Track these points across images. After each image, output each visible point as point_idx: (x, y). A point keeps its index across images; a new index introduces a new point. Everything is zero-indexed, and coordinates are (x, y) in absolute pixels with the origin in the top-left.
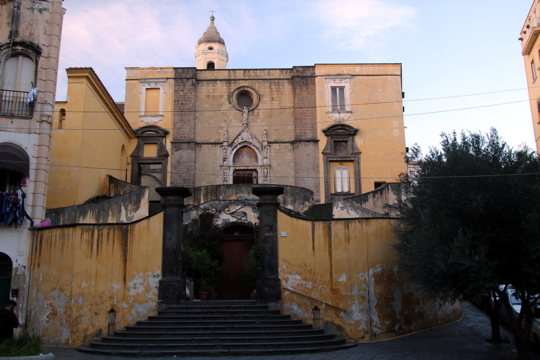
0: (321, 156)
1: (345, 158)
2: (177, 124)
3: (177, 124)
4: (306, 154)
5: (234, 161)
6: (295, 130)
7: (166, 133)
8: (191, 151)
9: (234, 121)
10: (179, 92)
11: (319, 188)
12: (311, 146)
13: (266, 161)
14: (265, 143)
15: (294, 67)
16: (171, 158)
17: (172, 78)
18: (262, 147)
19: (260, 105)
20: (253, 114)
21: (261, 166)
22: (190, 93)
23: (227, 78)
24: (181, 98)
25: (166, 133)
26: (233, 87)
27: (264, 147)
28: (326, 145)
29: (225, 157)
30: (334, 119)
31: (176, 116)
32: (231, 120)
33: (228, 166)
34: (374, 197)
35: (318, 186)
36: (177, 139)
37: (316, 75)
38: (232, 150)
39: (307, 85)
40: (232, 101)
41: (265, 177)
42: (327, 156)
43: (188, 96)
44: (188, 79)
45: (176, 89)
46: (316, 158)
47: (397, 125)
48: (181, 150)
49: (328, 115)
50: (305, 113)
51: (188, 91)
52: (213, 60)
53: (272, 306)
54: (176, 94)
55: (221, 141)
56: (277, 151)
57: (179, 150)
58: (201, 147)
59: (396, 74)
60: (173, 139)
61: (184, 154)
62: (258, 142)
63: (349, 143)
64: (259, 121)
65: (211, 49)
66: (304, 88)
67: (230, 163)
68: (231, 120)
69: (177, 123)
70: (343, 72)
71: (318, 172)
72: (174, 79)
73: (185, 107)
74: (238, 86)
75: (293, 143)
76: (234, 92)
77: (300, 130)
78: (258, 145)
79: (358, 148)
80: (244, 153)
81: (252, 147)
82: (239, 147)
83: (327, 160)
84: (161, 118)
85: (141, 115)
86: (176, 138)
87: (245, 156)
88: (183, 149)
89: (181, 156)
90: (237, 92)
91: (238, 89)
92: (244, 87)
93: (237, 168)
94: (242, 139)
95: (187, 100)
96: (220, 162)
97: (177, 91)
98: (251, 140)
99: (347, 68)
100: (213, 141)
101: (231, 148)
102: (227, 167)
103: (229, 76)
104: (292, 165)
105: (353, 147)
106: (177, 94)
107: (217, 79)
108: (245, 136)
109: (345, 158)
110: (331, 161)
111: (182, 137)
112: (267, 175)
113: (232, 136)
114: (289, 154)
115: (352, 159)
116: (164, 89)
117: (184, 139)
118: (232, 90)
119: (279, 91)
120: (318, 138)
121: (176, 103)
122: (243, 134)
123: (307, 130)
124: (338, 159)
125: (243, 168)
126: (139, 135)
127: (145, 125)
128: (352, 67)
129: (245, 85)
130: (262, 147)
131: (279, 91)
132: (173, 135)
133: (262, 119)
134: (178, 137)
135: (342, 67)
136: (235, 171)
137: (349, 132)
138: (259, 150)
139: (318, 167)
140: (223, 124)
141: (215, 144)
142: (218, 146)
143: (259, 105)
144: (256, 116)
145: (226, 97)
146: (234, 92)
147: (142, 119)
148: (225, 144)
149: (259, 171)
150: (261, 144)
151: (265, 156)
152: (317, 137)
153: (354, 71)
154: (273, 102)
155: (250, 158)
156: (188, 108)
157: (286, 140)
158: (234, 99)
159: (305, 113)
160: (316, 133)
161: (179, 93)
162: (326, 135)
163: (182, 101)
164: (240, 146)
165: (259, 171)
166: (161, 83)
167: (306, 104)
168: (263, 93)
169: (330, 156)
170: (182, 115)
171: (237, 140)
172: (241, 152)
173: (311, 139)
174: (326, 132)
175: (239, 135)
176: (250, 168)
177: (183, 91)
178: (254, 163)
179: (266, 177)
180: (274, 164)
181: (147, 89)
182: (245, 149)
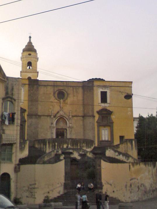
0: (96, 124)
16: (27, 122)
26: (56, 89)
38: (56, 119)
46: (93, 124)
52: (31, 61)
63: (109, 118)
65: (30, 55)
71: (94, 130)
78: (67, 117)
81: (64, 118)
82: (58, 118)
87: (61, 123)
91: (58, 90)
93: (57, 128)
98: (64, 115)
100: (46, 114)
105: (110, 119)
108: (61, 113)
118: (55, 91)
119: (77, 92)
120: (95, 115)
130: (69, 118)
131: (77, 92)
132: (28, 111)
139: (94, 128)
140: (51, 107)
141: (48, 116)
142: (49, 117)
145: (53, 94)
148: (52, 116)
150: (69, 117)
154: (74, 97)
158: (56, 95)
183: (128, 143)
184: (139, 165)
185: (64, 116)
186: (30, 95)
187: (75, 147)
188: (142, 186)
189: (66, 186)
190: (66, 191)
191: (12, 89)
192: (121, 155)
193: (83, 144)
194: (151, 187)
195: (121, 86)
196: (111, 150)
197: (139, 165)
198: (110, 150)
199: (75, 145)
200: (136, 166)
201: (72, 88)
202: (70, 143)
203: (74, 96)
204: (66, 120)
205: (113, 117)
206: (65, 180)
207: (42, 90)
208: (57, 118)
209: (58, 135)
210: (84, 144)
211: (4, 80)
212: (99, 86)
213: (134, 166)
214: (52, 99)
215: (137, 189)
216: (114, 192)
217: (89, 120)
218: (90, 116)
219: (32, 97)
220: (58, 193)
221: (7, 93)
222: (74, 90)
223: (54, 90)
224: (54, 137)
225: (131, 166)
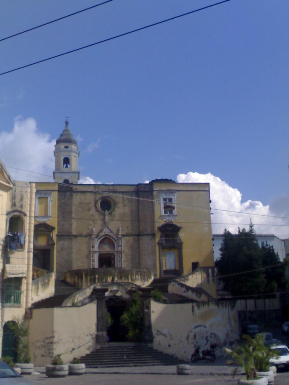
5: (99, 247)
7: (53, 228)
15: (138, 184)
25: (53, 228)
26: (98, 196)
27: (119, 239)
30: (165, 220)
35: (155, 265)
38: (98, 240)
52: (68, 157)
53: (149, 345)
65: (67, 147)
71: (155, 256)
78: (115, 238)
82: (102, 238)
91: (101, 198)
98: (111, 234)
108: (106, 231)
118: (97, 199)
130: (118, 238)
132: (58, 230)
138: (116, 241)
145: (93, 203)
164: (103, 238)
174: (160, 229)
184: (207, 305)
185: (110, 236)
186: (61, 206)
187: (125, 279)
188: (213, 336)
189: (98, 339)
190: (99, 347)
191: (22, 199)
192: (190, 292)
193: (136, 276)
194: (227, 337)
196: (175, 284)
197: (207, 305)
198: (174, 284)
199: (125, 277)
200: (202, 307)
202: (117, 275)
203: (125, 206)
205: (182, 235)
206: (98, 330)
207: (77, 199)
208: (100, 238)
209: (101, 264)
210: (137, 276)
211: (8, 187)
213: (199, 307)
214: (93, 211)
215: (205, 342)
216: (169, 346)
217: (145, 241)
220: (87, 349)
221: (14, 205)
224: (96, 265)
225: (196, 308)
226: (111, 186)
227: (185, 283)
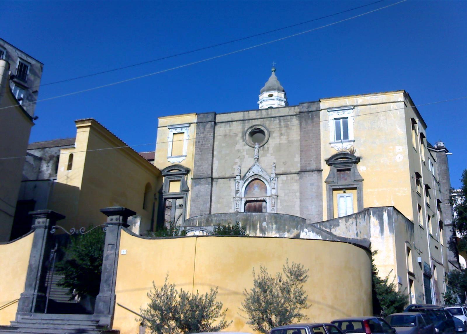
0: (324, 185)
1: (348, 185)
2: (197, 163)
3: (197, 163)
4: (310, 183)
6: (301, 161)
7: (188, 171)
8: (207, 185)
9: (246, 156)
10: (200, 134)
11: (323, 216)
12: (315, 175)
13: (274, 192)
14: (274, 175)
17: (195, 123)
18: (271, 179)
19: (270, 140)
20: (263, 150)
21: (270, 197)
22: (209, 135)
23: (242, 118)
24: (201, 139)
25: (188, 171)
26: (248, 125)
27: (272, 179)
28: (329, 174)
29: (238, 190)
30: (336, 148)
31: (197, 155)
32: (244, 156)
33: (239, 198)
34: (346, 221)
36: (197, 176)
37: (320, 109)
38: (244, 183)
39: (312, 118)
40: (245, 138)
41: (272, 207)
42: (330, 184)
43: (207, 137)
44: (208, 122)
45: (198, 132)
46: (320, 187)
47: (401, 151)
48: (199, 185)
49: (332, 145)
50: (310, 145)
51: (208, 133)
54: (197, 136)
55: (235, 175)
56: (285, 182)
57: (198, 185)
58: (217, 181)
59: (399, 100)
60: (194, 176)
61: (202, 189)
62: (267, 174)
64: (269, 155)
65: (271, 96)
66: (310, 121)
67: (242, 195)
68: (244, 156)
69: (197, 161)
70: (346, 103)
71: (321, 200)
72: (196, 123)
73: (205, 147)
74: (251, 125)
75: (299, 173)
76: (247, 130)
77: (305, 161)
78: (268, 178)
79: (360, 175)
80: (255, 185)
81: (262, 179)
82: (250, 180)
83: (329, 188)
84: (184, 158)
85: (168, 156)
86: (196, 174)
87: (257, 188)
88: (201, 184)
89: (199, 191)
90: (250, 130)
91: (251, 127)
92: (256, 125)
93: (248, 199)
94: (253, 173)
95: (206, 141)
96: (233, 194)
97: (199, 133)
98: (261, 174)
99: (350, 99)
100: (228, 175)
101: (243, 181)
102: (239, 199)
103: (244, 117)
104: (298, 194)
105: (356, 173)
106: (198, 136)
107: (234, 120)
108: (256, 170)
109: (348, 185)
110: (334, 190)
111: (200, 173)
112: (274, 205)
113: (244, 171)
114: (295, 184)
115: (355, 186)
116: (187, 132)
117: (202, 175)
118: (246, 129)
119: (287, 126)
120: (322, 168)
121: (197, 144)
122: (254, 168)
123: (311, 160)
124: (341, 187)
125: (253, 199)
126: (165, 173)
127: (171, 165)
128: (355, 99)
129: (257, 123)
130: (271, 179)
131: (287, 126)
133: (271, 153)
134: (198, 174)
135: (345, 100)
136: (247, 202)
137: (351, 160)
138: (268, 182)
140: (237, 160)
143: (269, 141)
144: (266, 150)
145: (240, 135)
146: (247, 130)
147: (169, 160)
149: (267, 201)
151: (273, 187)
152: (321, 167)
153: (357, 102)
154: (282, 137)
155: (261, 190)
156: (207, 147)
157: (293, 171)
159: (310, 145)
160: (320, 163)
161: (200, 135)
162: (329, 165)
163: (202, 142)
165: (268, 201)
166: (185, 128)
167: (311, 137)
168: (273, 130)
169: (333, 184)
170: (202, 154)
171: (248, 173)
172: (253, 184)
173: (316, 169)
174: (329, 162)
175: (250, 169)
176: (259, 199)
177: (203, 133)
178: (264, 195)
179: (274, 207)
180: (281, 194)
181: (174, 134)
182: (257, 181)
183: (371, 215)
195: (378, 102)
201: (277, 121)
203: (281, 134)
204: (265, 182)
212: (330, 110)
218: (313, 171)
219: (202, 144)
222: (282, 123)
223: (243, 128)
226: (264, 111)
227: (331, 230)
